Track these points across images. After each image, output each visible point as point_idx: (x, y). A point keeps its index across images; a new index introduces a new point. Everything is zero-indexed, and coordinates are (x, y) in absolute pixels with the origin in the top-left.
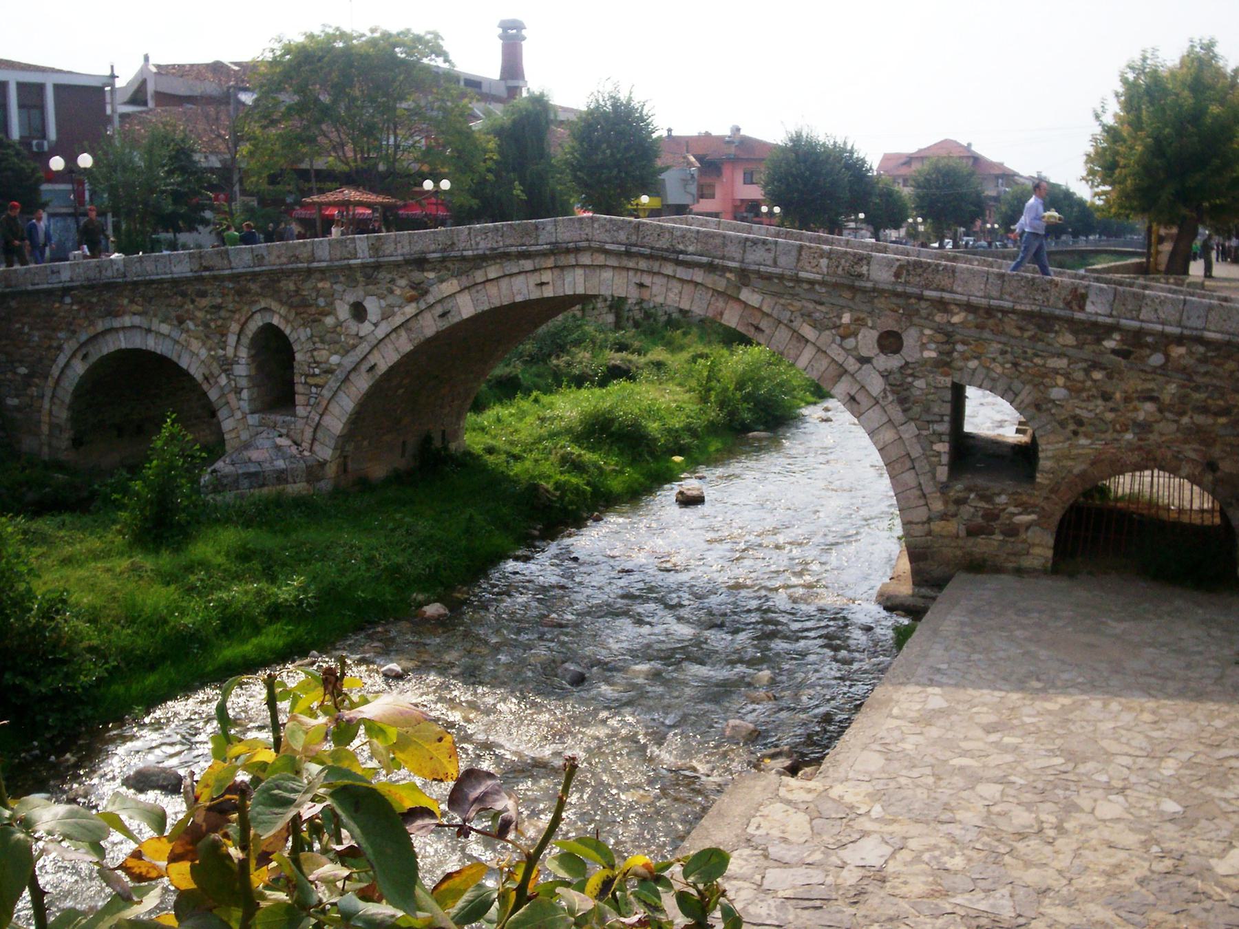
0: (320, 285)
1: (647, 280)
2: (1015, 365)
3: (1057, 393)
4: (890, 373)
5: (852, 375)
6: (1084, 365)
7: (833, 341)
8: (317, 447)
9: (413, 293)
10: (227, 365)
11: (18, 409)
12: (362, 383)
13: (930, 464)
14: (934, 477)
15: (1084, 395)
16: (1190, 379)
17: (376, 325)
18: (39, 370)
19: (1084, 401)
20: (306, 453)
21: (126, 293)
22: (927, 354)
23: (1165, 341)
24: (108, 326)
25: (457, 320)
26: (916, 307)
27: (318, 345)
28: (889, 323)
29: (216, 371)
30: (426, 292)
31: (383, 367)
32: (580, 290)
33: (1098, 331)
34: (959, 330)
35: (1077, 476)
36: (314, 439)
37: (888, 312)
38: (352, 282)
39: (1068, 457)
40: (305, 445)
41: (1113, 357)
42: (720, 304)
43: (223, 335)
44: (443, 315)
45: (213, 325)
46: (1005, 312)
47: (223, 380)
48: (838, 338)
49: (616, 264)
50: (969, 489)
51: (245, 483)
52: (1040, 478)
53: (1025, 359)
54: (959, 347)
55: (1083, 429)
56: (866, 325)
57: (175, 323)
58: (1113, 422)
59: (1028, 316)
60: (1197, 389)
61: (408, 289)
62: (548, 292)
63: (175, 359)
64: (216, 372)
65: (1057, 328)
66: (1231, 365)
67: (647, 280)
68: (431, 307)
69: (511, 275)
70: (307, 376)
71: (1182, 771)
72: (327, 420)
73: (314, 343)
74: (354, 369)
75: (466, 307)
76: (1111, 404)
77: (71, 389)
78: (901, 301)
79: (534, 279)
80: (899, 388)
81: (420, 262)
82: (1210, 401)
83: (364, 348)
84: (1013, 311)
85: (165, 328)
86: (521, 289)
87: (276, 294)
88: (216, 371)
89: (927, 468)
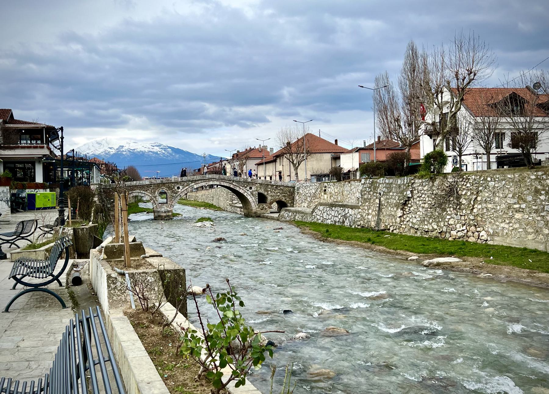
29: (153, 198)
33: (273, 185)
47: (154, 199)
81: (189, 181)
85: (143, 192)
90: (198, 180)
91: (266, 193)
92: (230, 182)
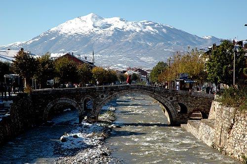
10: (80, 104)
33: (193, 97)
38: (102, 92)
91: (186, 104)
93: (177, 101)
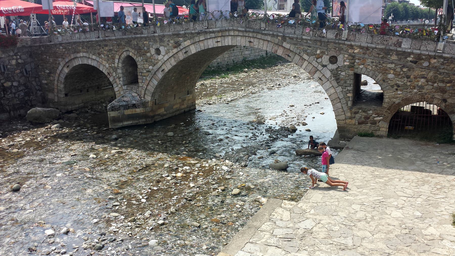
0: (145, 43)
1: (252, 40)
2: (376, 66)
3: (391, 76)
4: (333, 70)
5: (320, 71)
6: (400, 66)
7: (314, 60)
8: (146, 97)
9: (176, 45)
10: (115, 69)
11: (46, 84)
12: (160, 75)
13: (346, 101)
14: (347, 105)
15: (400, 76)
16: (438, 71)
17: (164, 56)
18: (53, 71)
19: (400, 78)
20: (142, 98)
21: (81, 45)
22: (345, 63)
23: (429, 57)
24: (75, 56)
25: (190, 54)
26: (342, 47)
27: (145, 63)
28: (333, 53)
29: (112, 71)
30: (180, 45)
31: (166, 70)
32: (230, 44)
33: (405, 54)
34: (357, 55)
35: (397, 104)
36: (145, 94)
37: (333, 49)
38: (155, 41)
39: (393, 98)
40: (142, 96)
41: (410, 63)
42: (276, 48)
43: (113, 59)
44: (186, 53)
45: (110, 56)
46: (373, 48)
48: (315, 59)
49: (242, 35)
50: (360, 109)
51: (122, 108)
52: (385, 105)
53: (380, 65)
54: (357, 61)
55: (399, 88)
56: (325, 54)
57: (98, 55)
58: (410, 85)
59: (381, 50)
60: (440, 74)
61: (174, 44)
62: (220, 45)
63: (98, 68)
64: (112, 72)
65: (391, 53)
66: (452, 66)
67: (252, 40)
68: (181, 50)
69: (207, 39)
70: (141, 73)
71: (424, 202)
72: (149, 87)
73: (144, 62)
74: (157, 71)
75: (193, 50)
76: (409, 80)
77: (64, 78)
78: (337, 45)
79: (215, 40)
80: (336, 75)
82: (444, 78)
83: (160, 63)
84: (376, 48)
85: (94, 57)
86: (211, 44)
87: (130, 46)
88: (112, 71)
89: (345, 102)
90: (199, 33)
92: (276, 41)
93: (352, 66)
